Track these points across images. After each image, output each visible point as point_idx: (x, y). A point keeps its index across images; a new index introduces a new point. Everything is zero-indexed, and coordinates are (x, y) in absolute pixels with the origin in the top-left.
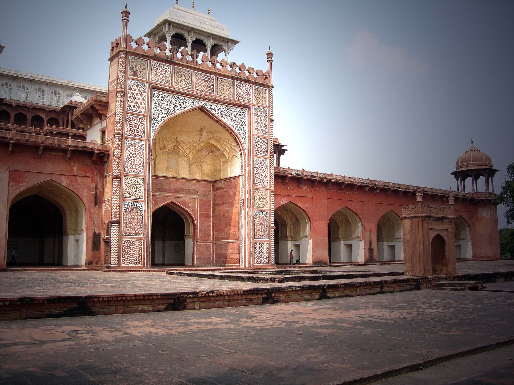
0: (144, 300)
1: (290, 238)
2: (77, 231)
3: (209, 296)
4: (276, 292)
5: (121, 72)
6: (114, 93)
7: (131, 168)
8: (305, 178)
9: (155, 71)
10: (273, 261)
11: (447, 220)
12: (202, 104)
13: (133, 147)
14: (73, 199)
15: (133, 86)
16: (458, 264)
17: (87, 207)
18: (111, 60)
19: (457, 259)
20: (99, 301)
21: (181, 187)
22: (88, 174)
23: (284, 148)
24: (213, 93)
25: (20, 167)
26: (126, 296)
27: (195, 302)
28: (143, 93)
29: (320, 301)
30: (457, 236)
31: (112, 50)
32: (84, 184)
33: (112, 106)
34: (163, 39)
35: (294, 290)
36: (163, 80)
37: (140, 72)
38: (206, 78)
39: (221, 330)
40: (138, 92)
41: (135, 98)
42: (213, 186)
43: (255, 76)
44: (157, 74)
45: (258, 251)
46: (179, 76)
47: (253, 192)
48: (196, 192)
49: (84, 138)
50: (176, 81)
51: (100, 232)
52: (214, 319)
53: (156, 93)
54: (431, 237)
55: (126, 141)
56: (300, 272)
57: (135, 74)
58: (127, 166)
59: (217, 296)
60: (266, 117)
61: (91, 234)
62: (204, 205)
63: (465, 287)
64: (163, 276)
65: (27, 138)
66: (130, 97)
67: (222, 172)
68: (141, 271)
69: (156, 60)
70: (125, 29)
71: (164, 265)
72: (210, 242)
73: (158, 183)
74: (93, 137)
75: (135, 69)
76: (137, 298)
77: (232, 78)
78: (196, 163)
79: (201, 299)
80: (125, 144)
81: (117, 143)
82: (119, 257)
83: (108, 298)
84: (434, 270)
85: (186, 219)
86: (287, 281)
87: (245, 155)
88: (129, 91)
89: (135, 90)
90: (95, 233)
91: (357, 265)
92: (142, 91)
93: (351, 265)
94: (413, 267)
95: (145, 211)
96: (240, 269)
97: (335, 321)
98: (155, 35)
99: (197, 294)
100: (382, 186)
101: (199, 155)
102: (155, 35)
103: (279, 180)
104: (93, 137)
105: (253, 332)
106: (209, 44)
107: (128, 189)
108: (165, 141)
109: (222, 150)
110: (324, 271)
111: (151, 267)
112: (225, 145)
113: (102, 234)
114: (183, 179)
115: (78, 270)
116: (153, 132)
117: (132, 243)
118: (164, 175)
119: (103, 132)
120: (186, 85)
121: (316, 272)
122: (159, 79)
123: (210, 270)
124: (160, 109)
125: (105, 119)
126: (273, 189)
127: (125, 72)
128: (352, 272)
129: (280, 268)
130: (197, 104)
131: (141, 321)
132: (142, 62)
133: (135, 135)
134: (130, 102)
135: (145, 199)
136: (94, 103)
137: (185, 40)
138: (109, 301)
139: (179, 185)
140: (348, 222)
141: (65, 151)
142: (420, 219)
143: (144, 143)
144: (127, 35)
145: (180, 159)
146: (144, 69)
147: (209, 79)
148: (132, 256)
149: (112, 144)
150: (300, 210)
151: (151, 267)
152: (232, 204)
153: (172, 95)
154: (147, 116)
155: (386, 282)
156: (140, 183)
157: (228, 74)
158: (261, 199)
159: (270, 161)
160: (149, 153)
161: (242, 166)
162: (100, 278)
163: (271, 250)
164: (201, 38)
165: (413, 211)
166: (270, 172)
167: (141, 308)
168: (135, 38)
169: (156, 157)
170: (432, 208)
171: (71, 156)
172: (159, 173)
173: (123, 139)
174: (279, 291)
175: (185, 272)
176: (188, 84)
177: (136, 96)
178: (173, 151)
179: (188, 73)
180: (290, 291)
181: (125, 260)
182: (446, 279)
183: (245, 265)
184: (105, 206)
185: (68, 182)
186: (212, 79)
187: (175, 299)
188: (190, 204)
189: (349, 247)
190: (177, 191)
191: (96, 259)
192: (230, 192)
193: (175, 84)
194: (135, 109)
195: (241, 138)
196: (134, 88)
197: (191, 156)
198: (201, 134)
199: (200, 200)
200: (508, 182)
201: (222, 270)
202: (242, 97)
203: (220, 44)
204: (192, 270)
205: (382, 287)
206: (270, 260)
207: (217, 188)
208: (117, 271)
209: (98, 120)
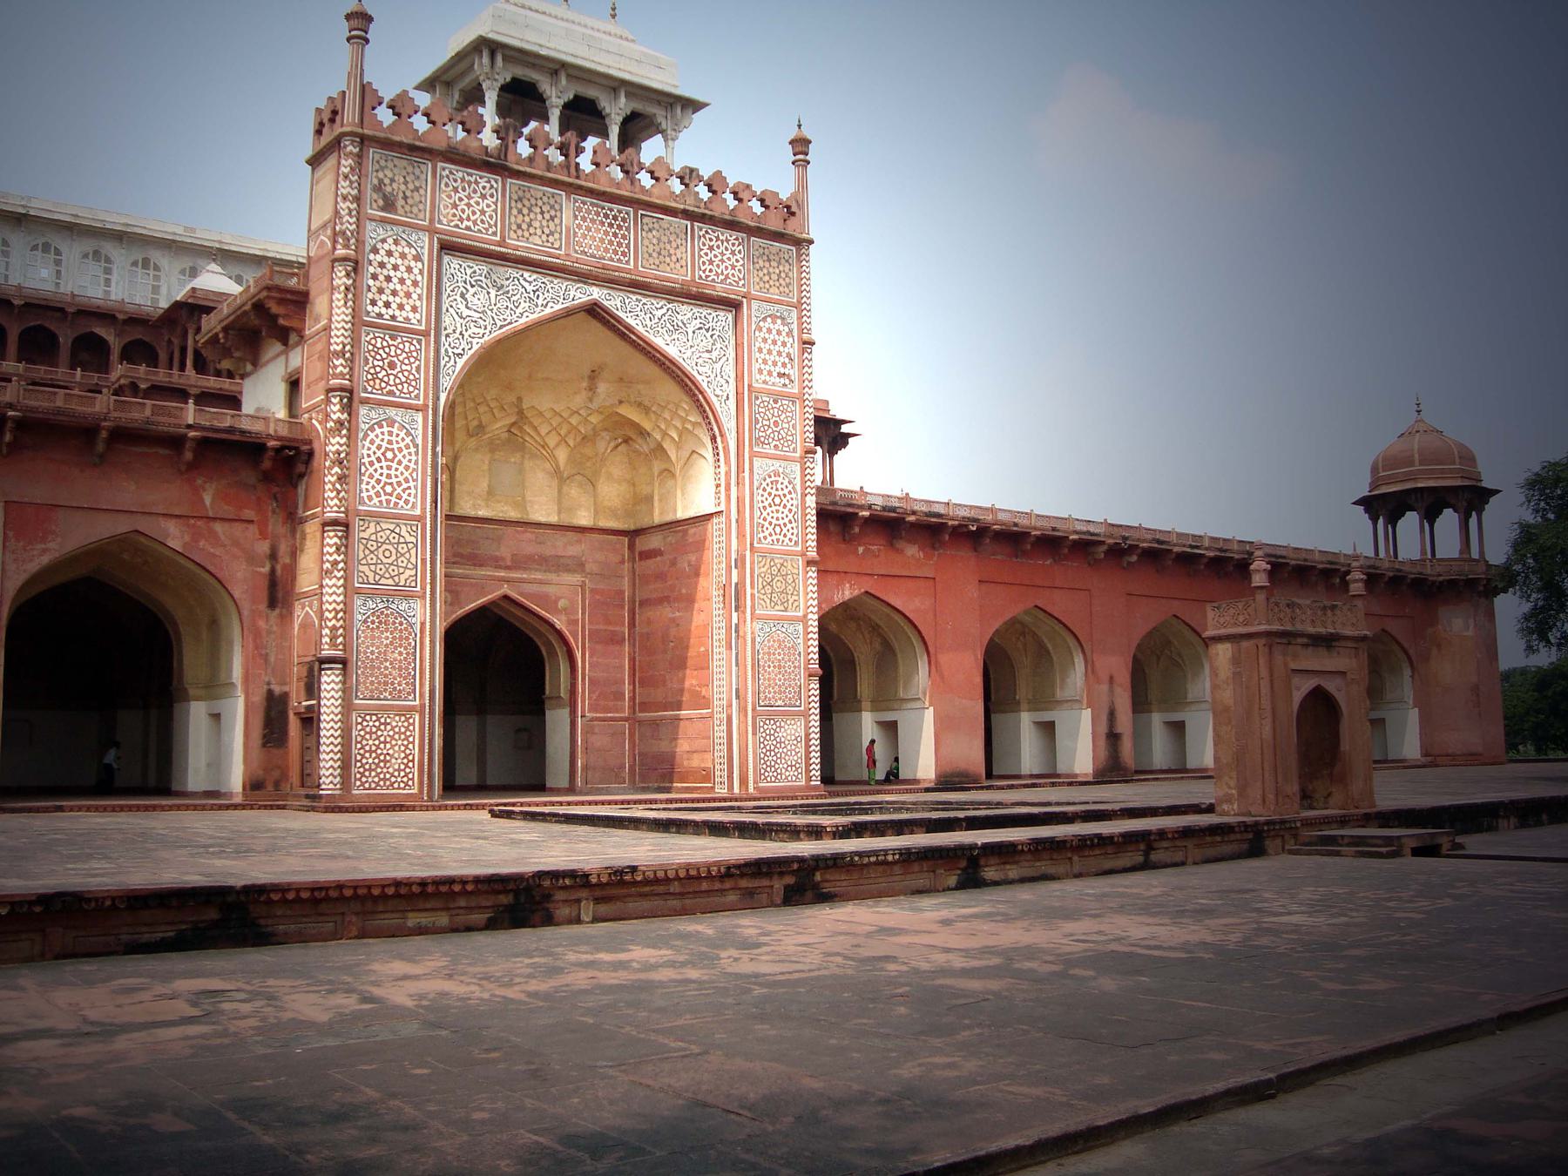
0: (424, 895)
1: (866, 704)
2: (215, 687)
3: (622, 883)
4: (827, 867)
5: (345, 198)
6: (326, 263)
7: (378, 494)
8: (912, 518)
9: (450, 197)
10: (816, 773)
11: (1343, 643)
13: (386, 429)
14: (202, 588)
15: (384, 241)
16: (1379, 777)
17: (246, 613)
18: (315, 161)
19: (1375, 762)
20: (284, 901)
21: (530, 549)
22: (248, 514)
23: (845, 429)
24: (628, 262)
25: (38, 492)
26: (369, 885)
27: (579, 901)
28: (413, 264)
29: (962, 896)
30: (1375, 693)
31: (319, 132)
32: (236, 543)
33: (319, 304)
34: (474, 96)
35: (880, 861)
36: (475, 223)
37: (405, 198)
38: (606, 216)
39: (661, 984)
40: (399, 262)
41: (388, 279)
42: (631, 547)
43: (757, 208)
44: (455, 206)
45: (770, 743)
46: (525, 211)
47: (752, 563)
48: (579, 566)
49: (234, 402)
50: (514, 227)
51: (286, 689)
52: (639, 954)
53: (452, 264)
54: (1297, 697)
55: (363, 410)
56: (900, 807)
58: (367, 488)
59: (646, 882)
60: (790, 333)
61: (259, 698)
62: (604, 603)
63: (1401, 846)
64: (480, 823)
65: (59, 403)
67: (656, 504)
68: (413, 808)
70: (358, 69)
71: (481, 788)
72: (622, 719)
73: (463, 540)
74: (263, 400)
75: (389, 189)
76: (403, 891)
77: (687, 215)
78: (578, 478)
79: (598, 893)
80: (361, 419)
81: (334, 417)
82: (346, 765)
83: (313, 890)
84: (1306, 797)
85: (549, 644)
86: (859, 836)
87: (726, 449)
88: (372, 256)
89: (389, 253)
90: (270, 693)
91: (1070, 784)
92: (410, 257)
93: (1053, 784)
94: (1242, 789)
95: (423, 624)
96: (714, 800)
97: (1009, 954)
98: (448, 85)
99: (586, 876)
100: (1144, 541)
101: (588, 451)
102: (448, 85)
103: (832, 527)
104: (263, 400)
105: (758, 991)
106: (616, 110)
108: (482, 409)
109: (658, 437)
110: (972, 803)
111: (442, 797)
112: (668, 421)
113: (293, 695)
114: (539, 525)
115: (221, 807)
116: (447, 382)
117: (386, 724)
118: (481, 513)
119: (294, 385)
120: (544, 237)
121: (946, 806)
122: (461, 220)
123: (622, 802)
124: (466, 312)
125: (297, 344)
126: (813, 554)
127: (357, 199)
128: (1058, 804)
129: (838, 795)
131: (415, 962)
132: (410, 169)
133: (391, 393)
134: (374, 290)
135: (423, 588)
136: (265, 293)
137: (541, 99)
138: (315, 902)
139: (526, 544)
140: (1042, 655)
141: (175, 442)
142: (1261, 642)
143: (419, 417)
144: (363, 87)
145: (528, 464)
146: (417, 189)
147: (615, 218)
148: (385, 761)
149: (322, 420)
150: (897, 617)
151: (442, 797)
152: (690, 600)
153: (502, 269)
154: (426, 334)
155: (1162, 834)
156: (409, 539)
157: (673, 204)
158: (778, 585)
159: (803, 469)
160: (434, 448)
161: (718, 486)
162: (287, 830)
163: (808, 739)
164: (590, 92)
165: (1241, 619)
166: (803, 501)
167: (413, 920)
168: (388, 94)
169: (456, 458)
170: (1300, 607)
171: (195, 457)
172: (466, 507)
173: (355, 404)
174: (835, 865)
175: (547, 810)
176: (552, 233)
177: (392, 273)
178: (509, 440)
179: (552, 201)
180: (870, 864)
181: (363, 775)
182: (1343, 821)
183: (731, 787)
184: (301, 611)
185: (187, 538)
186: (624, 220)
187: (517, 893)
188: (561, 604)
189: (1048, 729)
190: (519, 563)
191: (276, 774)
192: (683, 564)
193: (513, 235)
194: (391, 312)
196: (386, 246)
197: (562, 455)
198: (592, 389)
199: (592, 591)
200: (1529, 526)
201: (661, 802)
203: (651, 112)
204: (569, 804)
205: (1150, 848)
206: (808, 771)
207: (641, 554)
208: (341, 810)
209: (278, 347)
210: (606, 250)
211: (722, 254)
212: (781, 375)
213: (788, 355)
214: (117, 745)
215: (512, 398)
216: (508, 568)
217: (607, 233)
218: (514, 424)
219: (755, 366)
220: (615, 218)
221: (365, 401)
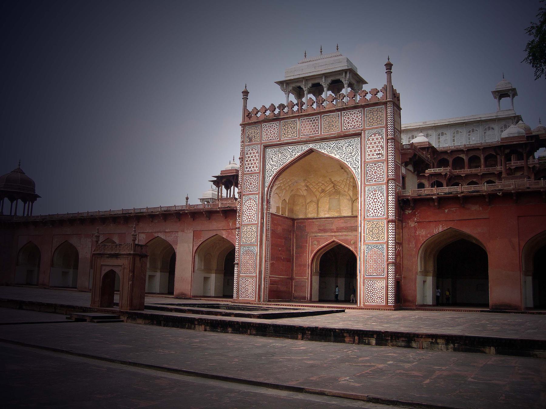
12: (311, 147)
21: (342, 225)
25: (199, 228)
41: (250, 160)
45: (370, 289)
47: (364, 224)
53: (269, 150)
54: (103, 273)
57: (251, 140)
58: (245, 218)
60: (382, 138)
66: (247, 161)
69: (266, 122)
77: (338, 110)
95: (257, 253)
107: (245, 236)
114: (345, 217)
116: (267, 184)
118: (327, 216)
130: (306, 148)
133: (251, 191)
158: (375, 231)
164: (316, 81)
169: (318, 201)
178: (335, 192)
186: (317, 120)
190: (339, 230)
195: (353, 169)
202: (351, 126)
210: (311, 132)
211: (353, 118)
212: (377, 154)
213: (381, 146)
214: (337, 286)
215: (328, 179)
216: (335, 232)
217: (311, 126)
218: (334, 186)
219: (367, 155)
220: (314, 120)
221: (244, 195)
